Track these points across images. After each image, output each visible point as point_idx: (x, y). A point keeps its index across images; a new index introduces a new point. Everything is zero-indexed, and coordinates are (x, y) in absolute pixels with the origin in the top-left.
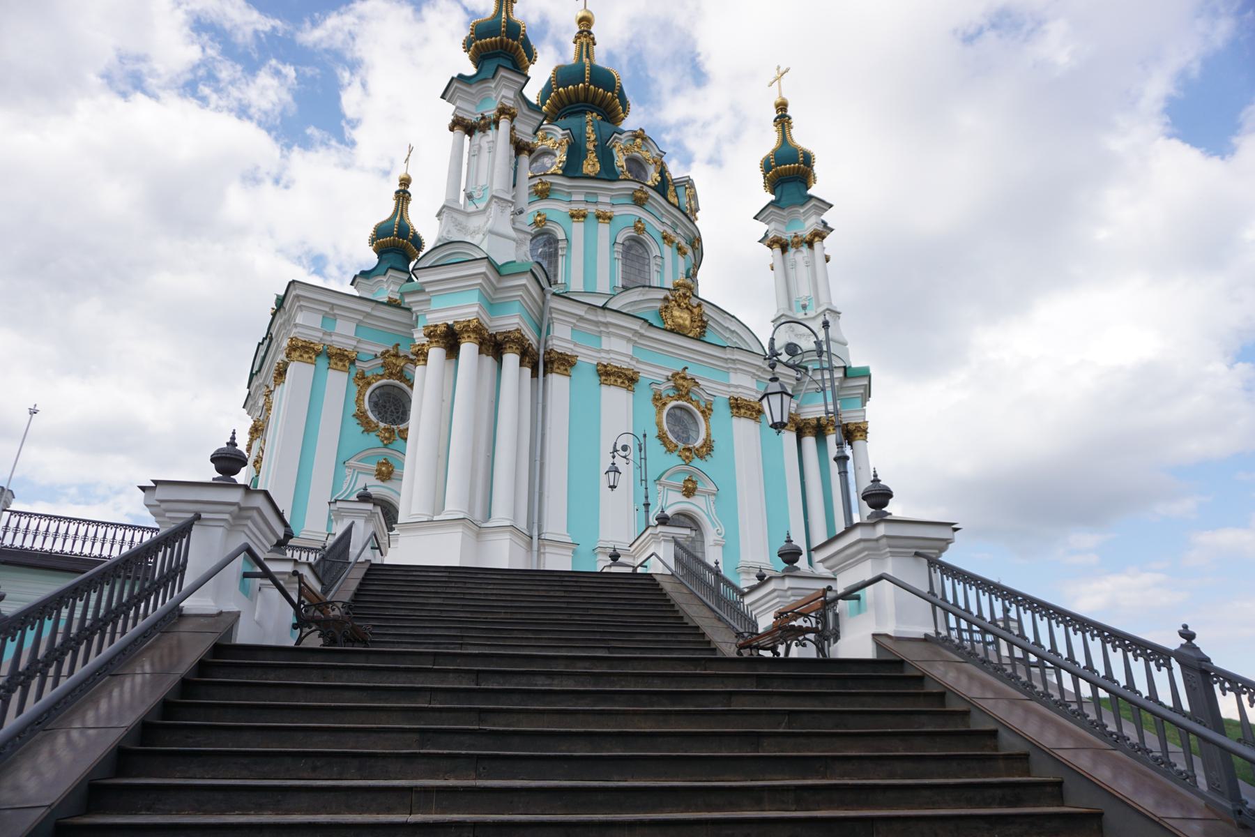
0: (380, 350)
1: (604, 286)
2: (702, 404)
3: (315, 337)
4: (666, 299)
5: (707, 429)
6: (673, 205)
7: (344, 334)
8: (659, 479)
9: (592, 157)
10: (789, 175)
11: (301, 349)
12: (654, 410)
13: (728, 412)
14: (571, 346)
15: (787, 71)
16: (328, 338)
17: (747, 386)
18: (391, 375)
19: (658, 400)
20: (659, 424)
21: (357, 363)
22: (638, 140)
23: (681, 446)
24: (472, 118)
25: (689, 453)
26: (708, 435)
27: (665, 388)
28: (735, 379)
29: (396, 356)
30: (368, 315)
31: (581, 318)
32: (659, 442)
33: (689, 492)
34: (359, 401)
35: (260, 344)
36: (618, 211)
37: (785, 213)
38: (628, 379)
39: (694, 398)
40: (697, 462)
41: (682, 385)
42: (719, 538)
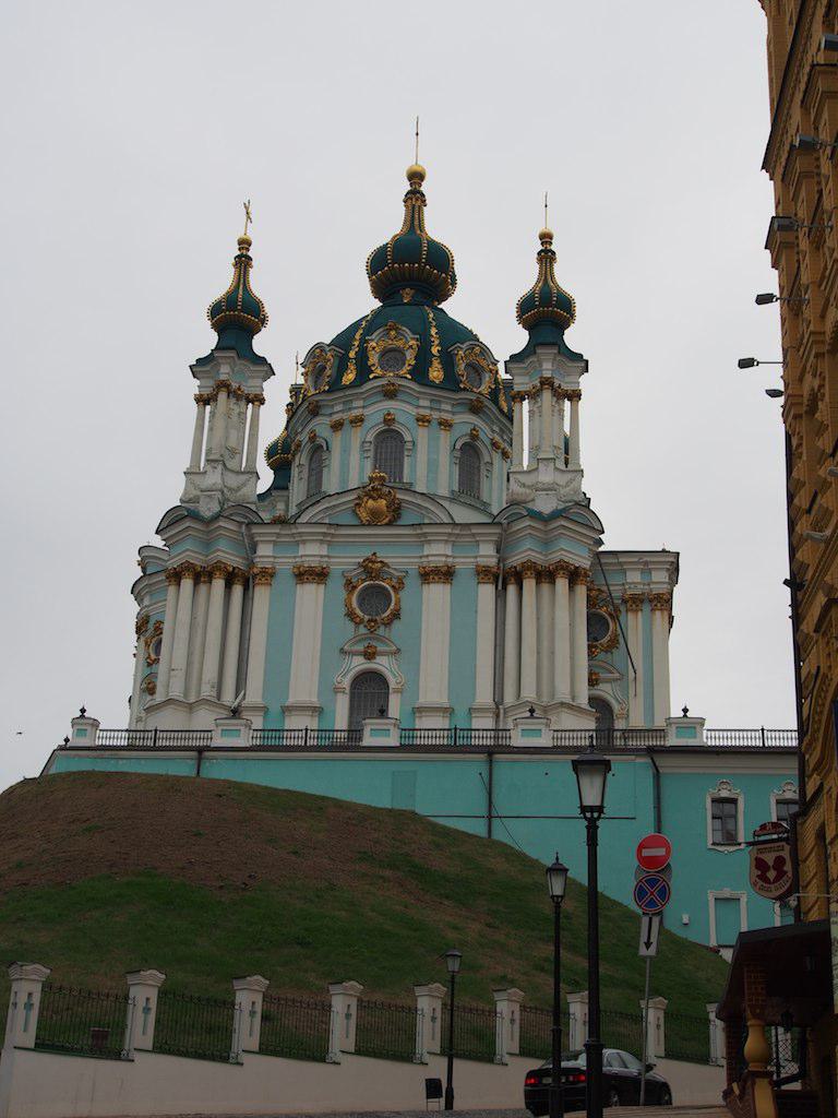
6: (431, 385)
10: (546, 313)
12: (343, 594)
14: (272, 560)
17: (438, 553)
19: (350, 586)
20: (348, 604)
22: (393, 333)
25: (372, 624)
27: (355, 573)
28: (427, 550)
31: (278, 535)
33: (370, 655)
38: (319, 575)
40: (381, 631)
41: (371, 568)
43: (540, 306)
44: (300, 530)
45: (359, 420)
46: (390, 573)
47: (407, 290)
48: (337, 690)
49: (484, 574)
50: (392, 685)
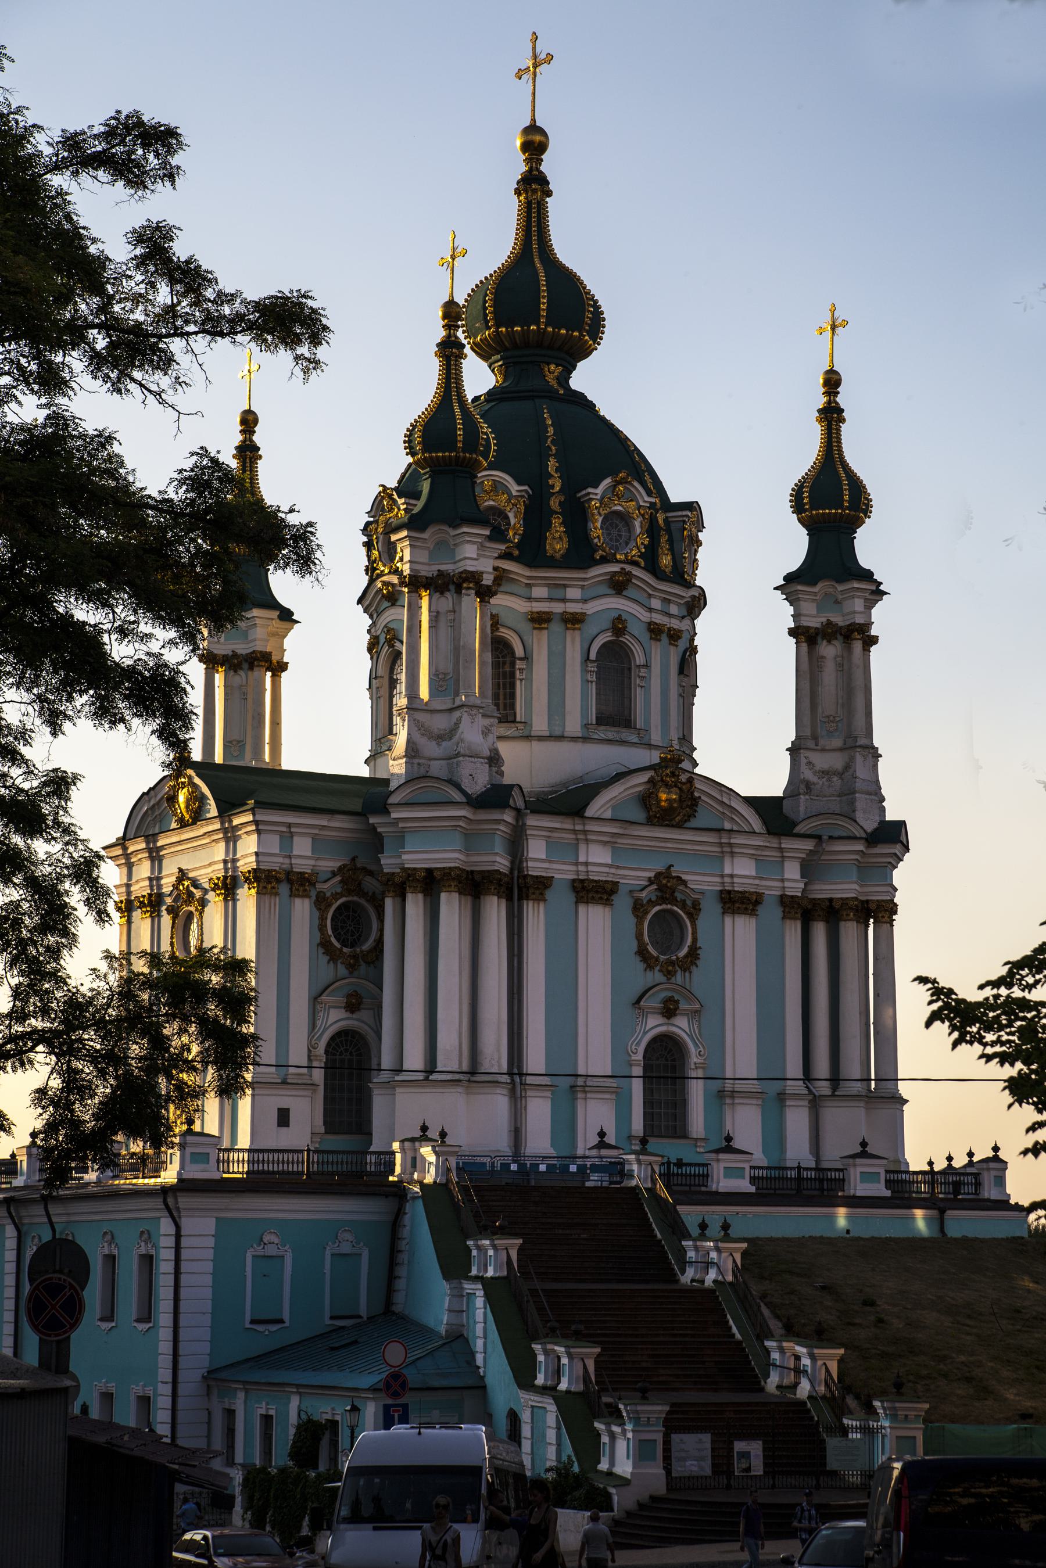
0: (338, 864)
1: (573, 725)
2: (689, 903)
3: (276, 863)
4: (651, 781)
5: (694, 933)
7: (303, 854)
8: (638, 1001)
9: (558, 526)
11: (264, 879)
12: (633, 920)
13: (718, 908)
14: (546, 865)
15: (845, 323)
16: (287, 861)
17: (742, 871)
18: (350, 892)
19: (639, 909)
20: (639, 936)
21: (319, 886)
23: (662, 958)
24: (427, 571)
26: (695, 940)
29: (355, 869)
30: (323, 827)
32: (638, 958)
33: (669, 1010)
34: (322, 928)
35: (144, 794)
36: (592, 608)
37: (816, 589)
39: (679, 896)
40: (679, 978)
41: (667, 885)
42: (700, 1060)
43: (848, 508)
44: (588, 828)
45: (573, 621)
46: (683, 892)
47: (552, 367)
48: (631, 1065)
49: (789, 905)
50: (694, 1059)
